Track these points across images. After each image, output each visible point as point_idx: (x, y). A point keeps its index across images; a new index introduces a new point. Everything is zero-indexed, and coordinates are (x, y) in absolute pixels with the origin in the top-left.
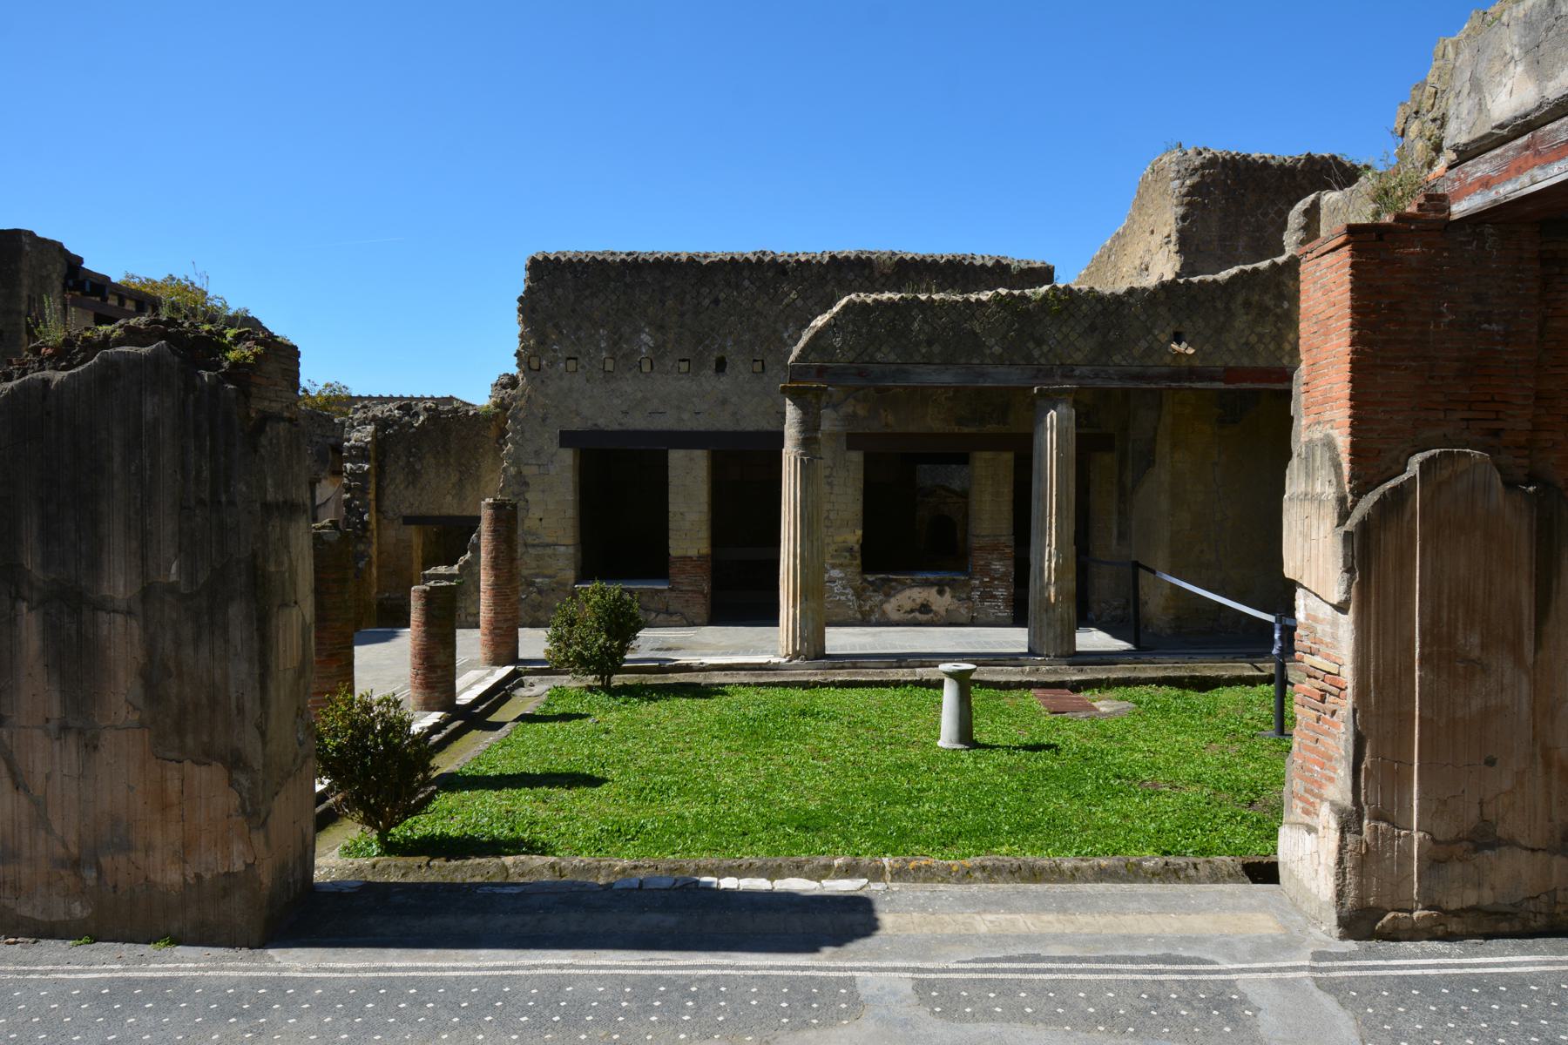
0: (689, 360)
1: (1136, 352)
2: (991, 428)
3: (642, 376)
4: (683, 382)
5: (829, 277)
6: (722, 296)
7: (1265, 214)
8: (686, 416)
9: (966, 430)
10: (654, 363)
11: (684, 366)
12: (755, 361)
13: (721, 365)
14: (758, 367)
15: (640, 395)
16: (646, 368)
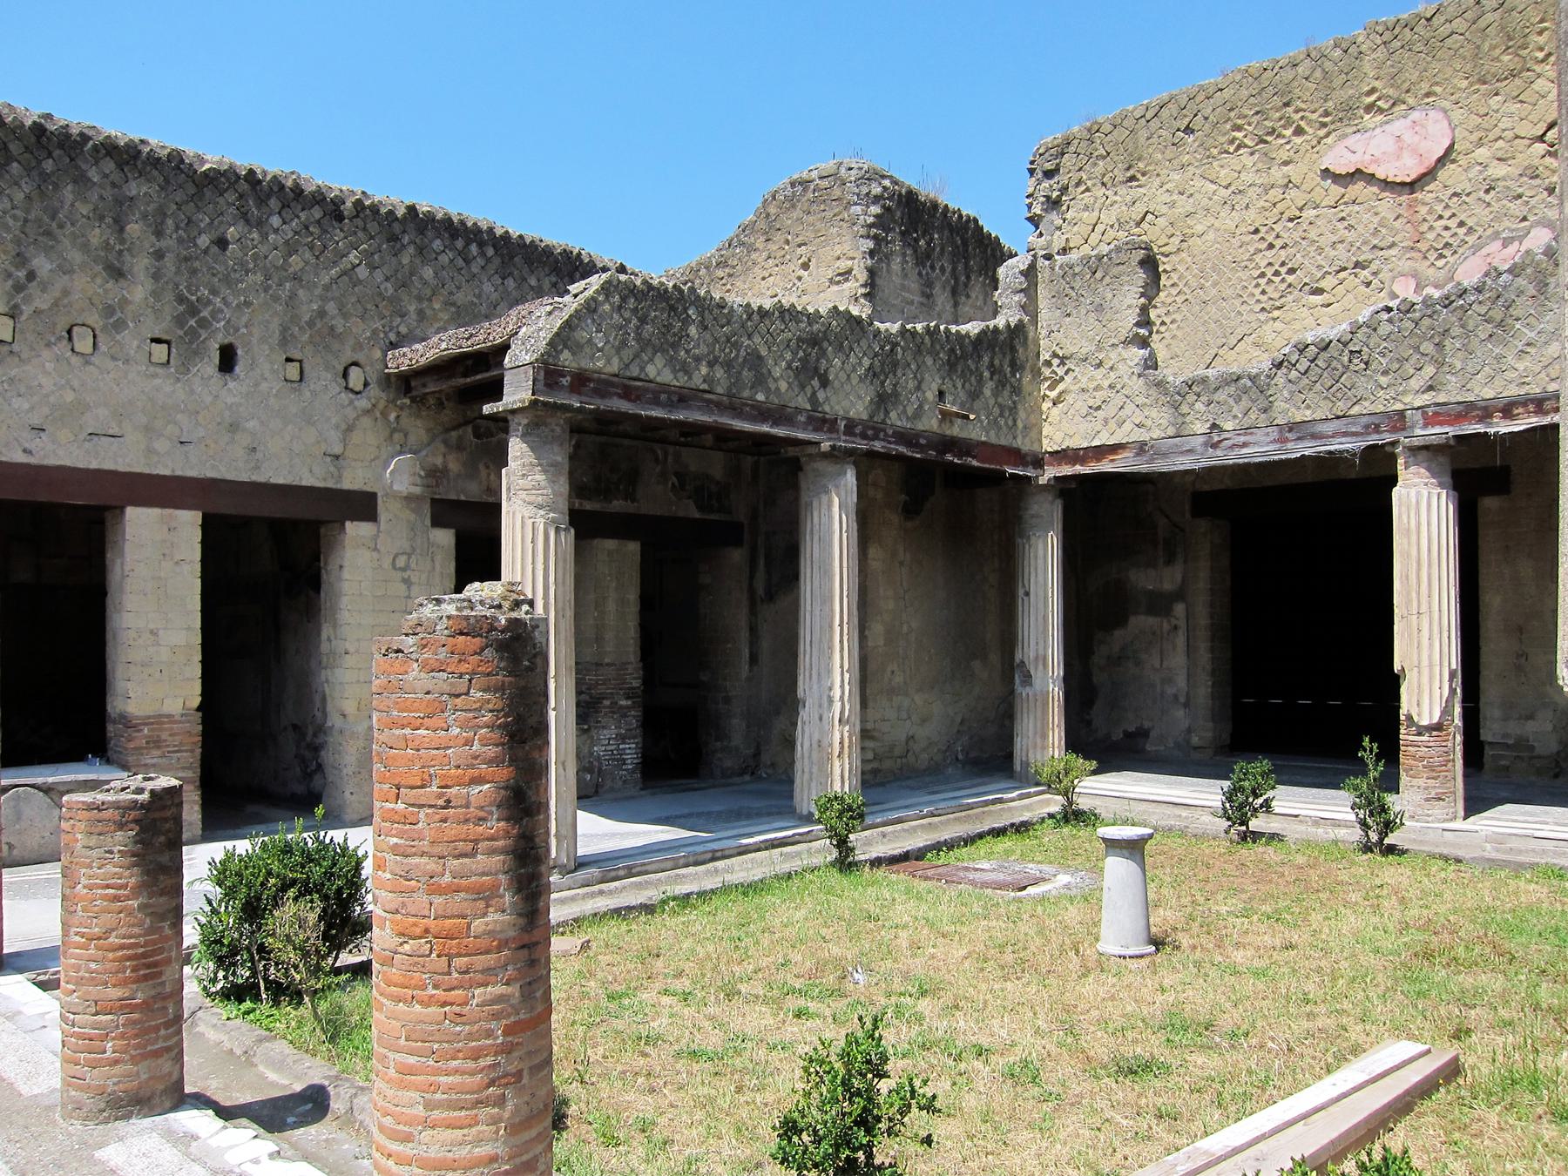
0: (168, 342)
1: (910, 412)
2: (617, 505)
3: (75, 360)
4: (158, 381)
5: (406, 239)
6: (232, 232)
7: (933, 267)
8: (161, 445)
10: (101, 338)
11: (160, 351)
12: (288, 360)
13: (227, 360)
14: (293, 371)
15: (70, 396)
16: (84, 344)
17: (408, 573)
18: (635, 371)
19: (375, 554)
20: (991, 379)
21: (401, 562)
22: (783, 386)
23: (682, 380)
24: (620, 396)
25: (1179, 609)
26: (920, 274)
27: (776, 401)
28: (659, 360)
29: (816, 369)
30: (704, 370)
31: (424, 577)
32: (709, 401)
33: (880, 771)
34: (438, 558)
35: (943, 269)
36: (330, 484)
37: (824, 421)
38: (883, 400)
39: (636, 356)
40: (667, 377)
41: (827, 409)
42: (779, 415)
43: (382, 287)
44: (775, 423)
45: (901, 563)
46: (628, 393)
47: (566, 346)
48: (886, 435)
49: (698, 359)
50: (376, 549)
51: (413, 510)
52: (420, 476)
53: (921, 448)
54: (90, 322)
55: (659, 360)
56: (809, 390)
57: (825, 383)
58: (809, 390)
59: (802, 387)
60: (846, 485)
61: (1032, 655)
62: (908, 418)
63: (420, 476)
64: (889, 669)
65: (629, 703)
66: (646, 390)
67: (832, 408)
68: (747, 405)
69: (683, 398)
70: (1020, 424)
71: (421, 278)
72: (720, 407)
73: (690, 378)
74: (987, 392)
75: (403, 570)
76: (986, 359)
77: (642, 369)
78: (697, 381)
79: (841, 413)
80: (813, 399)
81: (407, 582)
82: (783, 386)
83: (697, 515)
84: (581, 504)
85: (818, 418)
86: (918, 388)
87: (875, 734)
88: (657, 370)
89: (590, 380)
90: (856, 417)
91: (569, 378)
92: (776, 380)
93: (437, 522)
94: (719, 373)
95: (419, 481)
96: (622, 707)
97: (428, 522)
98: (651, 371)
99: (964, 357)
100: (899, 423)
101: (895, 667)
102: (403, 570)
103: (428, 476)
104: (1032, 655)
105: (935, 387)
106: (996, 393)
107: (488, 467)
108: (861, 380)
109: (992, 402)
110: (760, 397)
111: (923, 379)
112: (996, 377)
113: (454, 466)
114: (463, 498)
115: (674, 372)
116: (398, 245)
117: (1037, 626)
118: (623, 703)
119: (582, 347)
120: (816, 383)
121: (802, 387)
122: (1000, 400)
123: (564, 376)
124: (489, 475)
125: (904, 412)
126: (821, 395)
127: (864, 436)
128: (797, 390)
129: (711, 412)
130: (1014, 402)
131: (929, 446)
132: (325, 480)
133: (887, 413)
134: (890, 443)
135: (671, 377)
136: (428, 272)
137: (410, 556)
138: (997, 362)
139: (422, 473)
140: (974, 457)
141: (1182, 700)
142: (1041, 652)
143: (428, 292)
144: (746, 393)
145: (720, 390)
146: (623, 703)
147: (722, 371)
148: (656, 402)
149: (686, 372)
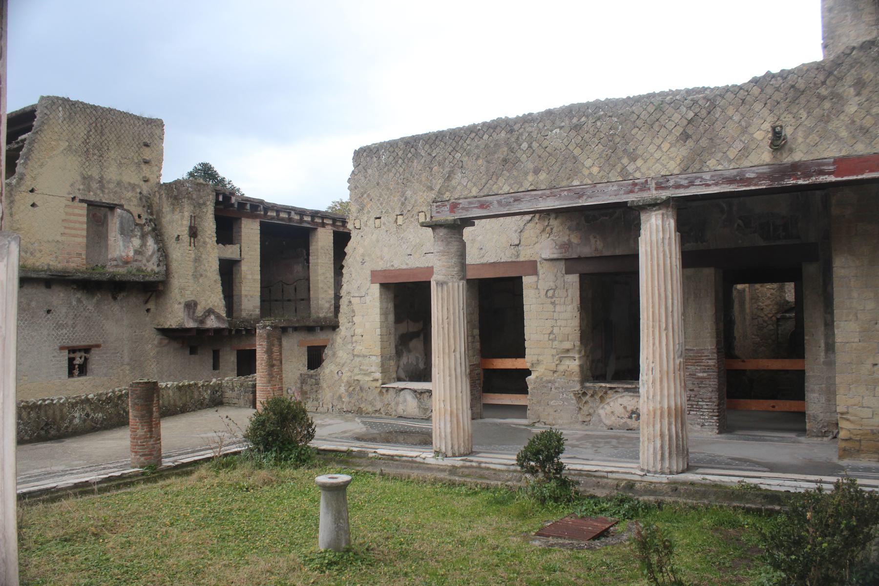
1: (732, 154)
17: (554, 299)
21: (550, 293)
31: (562, 300)
34: (570, 292)
36: (514, 259)
37: (635, 185)
41: (638, 175)
49: (526, 174)
54: (423, 210)
65: (705, 375)
67: (643, 174)
68: (565, 190)
87: (848, 417)
93: (568, 272)
97: (564, 272)
105: (767, 126)
107: (595, 237)
110: (576, 183)
113: (575, 240)
118: (700, 375)
120: (625, 161)
124: (596, 241)
126: (631, 168)
132: (511, 257)
137: (554, 290)
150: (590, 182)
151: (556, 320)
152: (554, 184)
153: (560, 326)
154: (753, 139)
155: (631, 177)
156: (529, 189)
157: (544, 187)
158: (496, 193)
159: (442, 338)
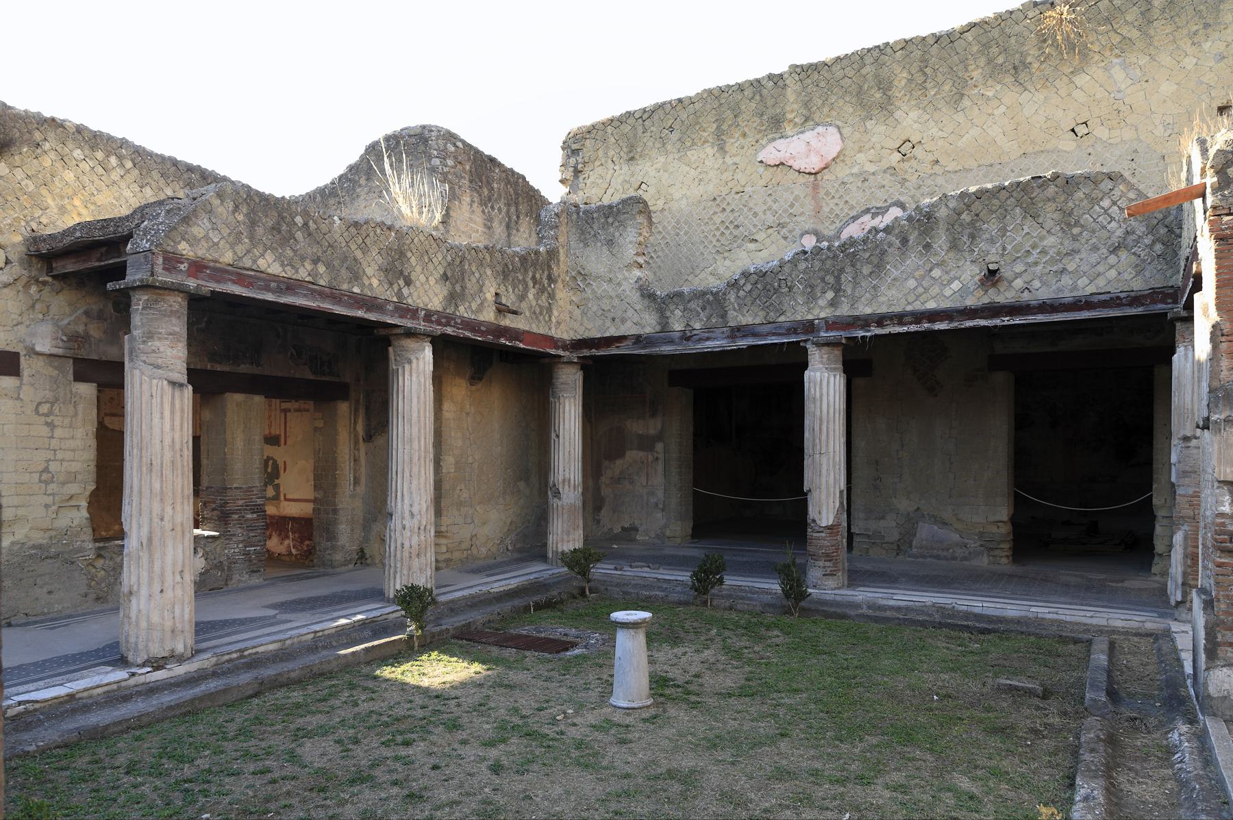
1: (474, 306)
7: (492, 208)
9: (219, 368)
17: (52, 418)
18: (248, 263)
19: (18, 403)
20: (534, 287)
21: (44, 408)
22: (375, 282)
23: (289, 273)
24: (234, 282)
25: (659, 446)
26: (483, 212)
27: (370, 294)
28: (269, 256)
29: (401, 272)
30: (309, 266)
31: (67, 421)
32: (313, 291)
33: (451, 560)
34: (80, 408)
35: (500, 210)
37: (408, 310)
38: (453, 298)
39: (248, 252)
40: (275, 269)
41: (410, 301)
42: (372, 303)
43: (23, 183)
44: (369, 310)
45: (468, 414)
46: (241, 279)
47: (184, 239)
48: (456, 323)
49: (303, 259)
50: (18, 398)
51: (56, 368)
52: (62, 340)
53: (482, 333)
55: (269, 256)
56: (396, 287)
57: (408, 282)
58: (396, 287)
59: (391, 284)
60: (424, 358)
61: (561, 478)
62: (472, 311)
63: (62, 340)
64: (458, 488)
65: (255, 516)
66: (259, 279)
67: (414, 301)
68: (346, 295)
69: (290, 286)
70: (554, 320)
71: (62, 179)
72: (322, 295)
73: (297, 272)
74: (531, 296)
75: (47, 415)
76: (530, 274)
77: (255, 262)
78: (303, 274)
79: (421, 305)
80: (399, 293)
81: (51, 425)
82: (375, 282)
83: (312, 377)
84: (212, 366)
85: (403, 308)
86: (481, 290)
88: (269, 264)
89: (207, 267)
90: (433, 309)
91: (186, 265)
92: (369, 278)
93: (79, 377)
94: (321, 269)
95: (61, 344)
96: (247, 520)
97: (71, 377)
98: (262, 264)
99: (515, 270)
100: (466, 315)
101: (463, 487)
102: (47, 415)
103: (69, 340)
104: (561, 478)
105: (493, 291)
106: (537, 297)
108: (437, 282)
109: (534, 303)
110: (356, 290)
111: (484, 284)
112: (537, 286)
114: (104, 358)
115: (282, 265)
116: (39, 151)
117: (564, 459)
118: (249, 516)
119: (199, 240)
120: (401, 282)
121: (391, 284)
122: (540, 302)
123: (182, 263)
125: (470, 307)
126: (405, 291)
127: (439, 323)
128: (386, 286)
129: (314, 299)
130: (550, 304)
131: (488, 332)
133: (457, 306)
134: (458, 329)
135: (280, 269)
136: (69, 176)
137: (52, 404)
138: (538, 276)
139: (65, 338)
140: (521, 341)
141: (661, 506)
142: (567, 476)
143: (70, 191)
144: (345, 287)
145: (322, 282)
146: (249, 516)
147: (324, 268)
148: (267, 289)
149: (293, 267)
150: (370, 294)
151: (55, 450)
152: (334, 284)
153: (62, 460)
154: (486, 299)
155: (405, 302)
156: (306, 280)
157: (324, 284)
158: (263, 269)
159: (179, 471)
